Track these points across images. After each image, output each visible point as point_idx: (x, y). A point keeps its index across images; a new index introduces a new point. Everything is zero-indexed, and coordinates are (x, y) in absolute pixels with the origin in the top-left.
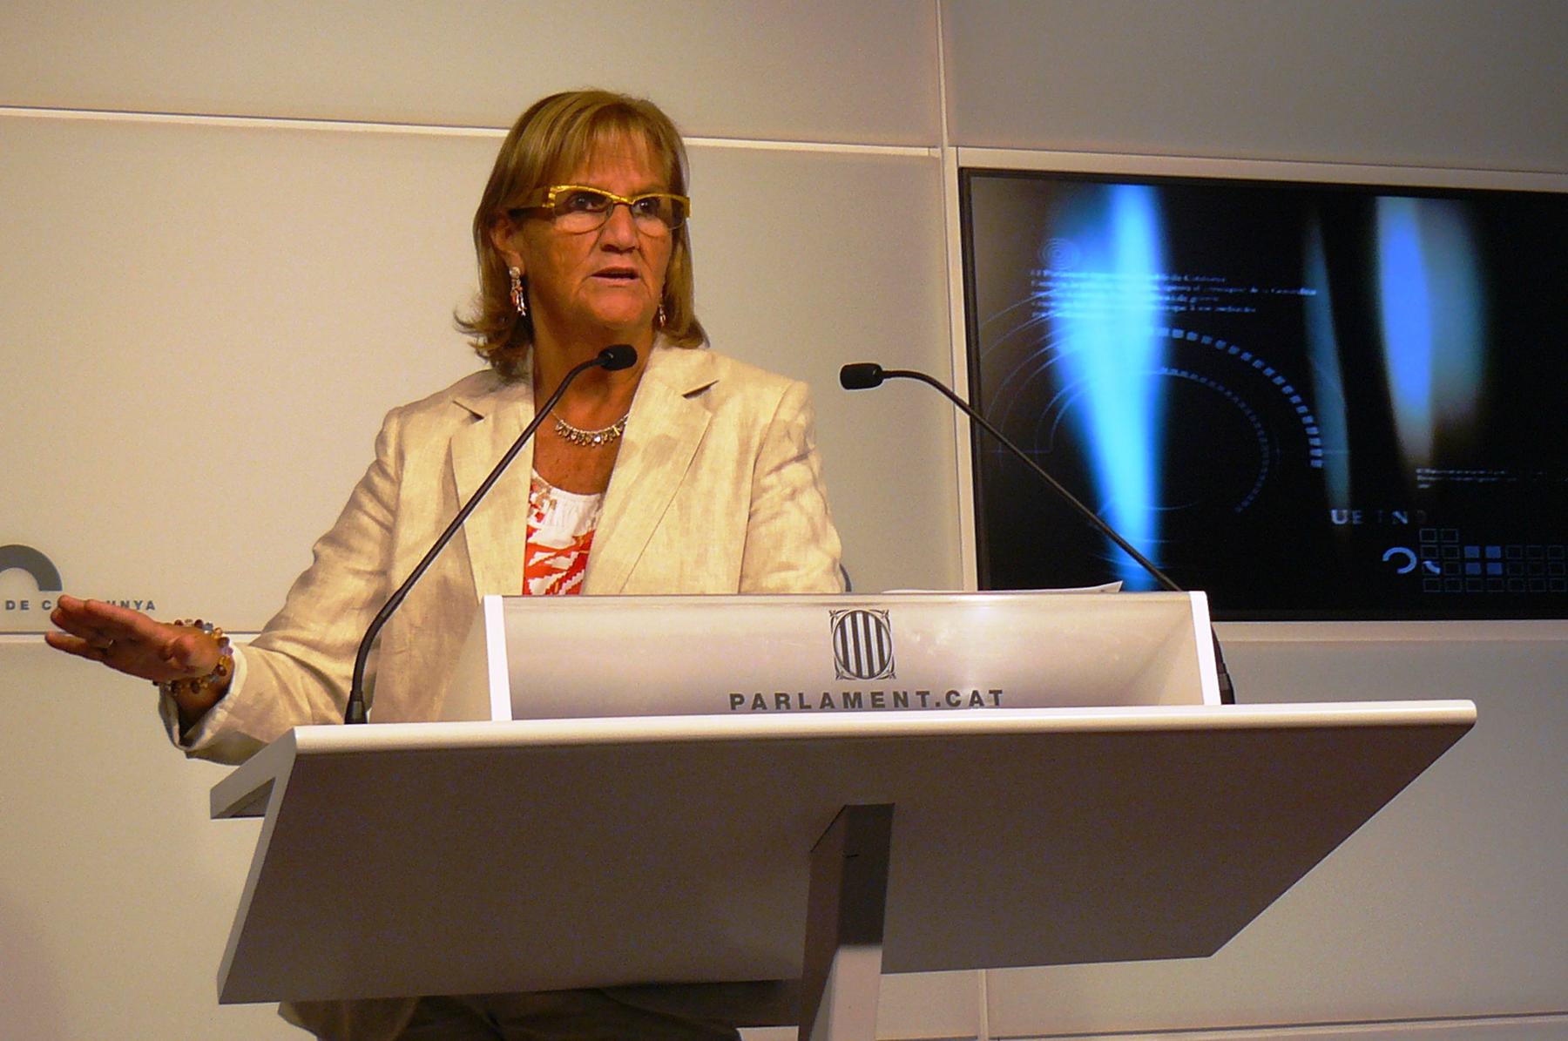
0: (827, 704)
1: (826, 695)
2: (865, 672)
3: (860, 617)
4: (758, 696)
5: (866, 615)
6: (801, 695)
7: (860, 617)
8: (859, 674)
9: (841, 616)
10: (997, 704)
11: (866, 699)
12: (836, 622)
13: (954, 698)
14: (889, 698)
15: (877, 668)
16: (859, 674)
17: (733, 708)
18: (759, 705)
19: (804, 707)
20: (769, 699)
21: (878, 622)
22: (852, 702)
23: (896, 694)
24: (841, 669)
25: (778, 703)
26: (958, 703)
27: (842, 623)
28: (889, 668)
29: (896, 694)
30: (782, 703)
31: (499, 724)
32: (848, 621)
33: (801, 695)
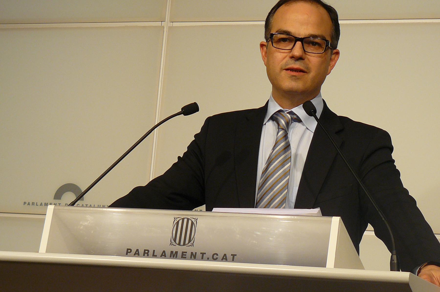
0: (163, 255)
1: (164, 252)
2: (182, 243)
3: (185, 220)
4: (137, 250)
5: (188, 220)
6: (154, 251)
7: (185, 220)
8: (179, 244)
10: (233, 260)
11: (180, 254)
13: (215, 257)
14: (188, 255)
15: (187, 242)
16: (179, 244)
17: (127, 254)
18: (137, 254)
19: (154, 256)
20: (141, 252)
21: (192, 223)
22: (174, 255)
23: (192, 253)
24: (173, 241)
25: (145, 253)
26: (217, 258)
27: (178, 223)
28: (192, 242)
29: (192, 253)
30: (146, 253)
31: (42, 254)
32: (180, 222)
33: (154, 251)
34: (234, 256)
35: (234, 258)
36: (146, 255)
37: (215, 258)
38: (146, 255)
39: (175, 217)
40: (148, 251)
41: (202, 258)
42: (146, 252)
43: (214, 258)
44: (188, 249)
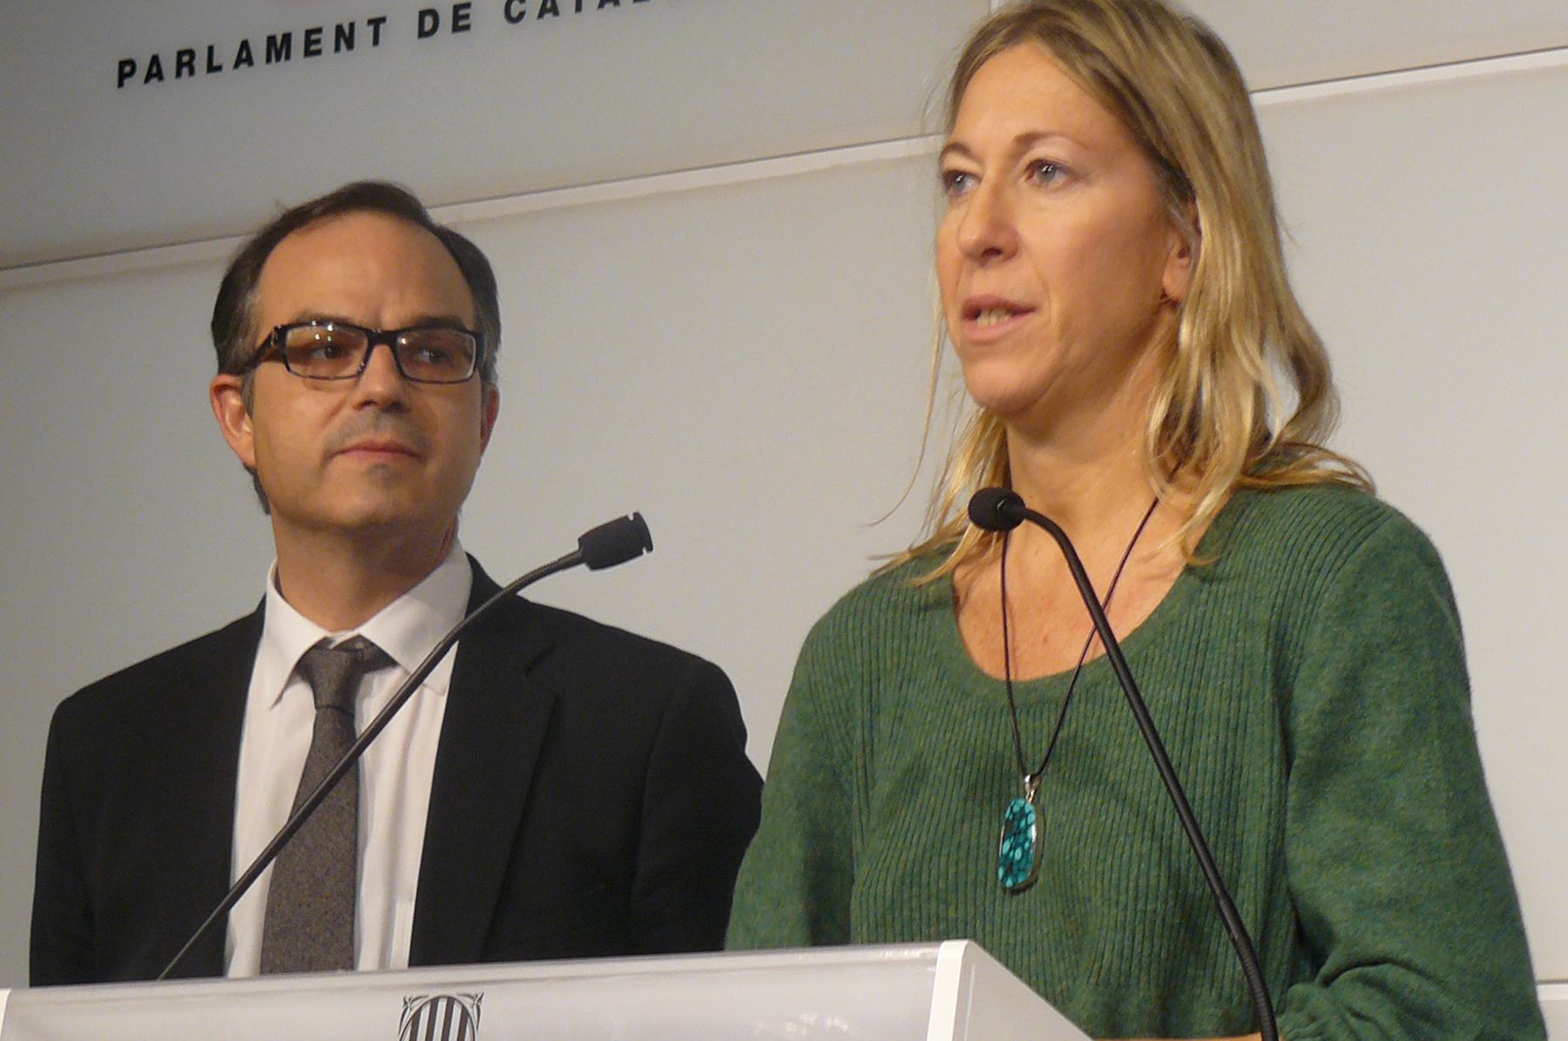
23: (339, 29)
42: (186, 59)
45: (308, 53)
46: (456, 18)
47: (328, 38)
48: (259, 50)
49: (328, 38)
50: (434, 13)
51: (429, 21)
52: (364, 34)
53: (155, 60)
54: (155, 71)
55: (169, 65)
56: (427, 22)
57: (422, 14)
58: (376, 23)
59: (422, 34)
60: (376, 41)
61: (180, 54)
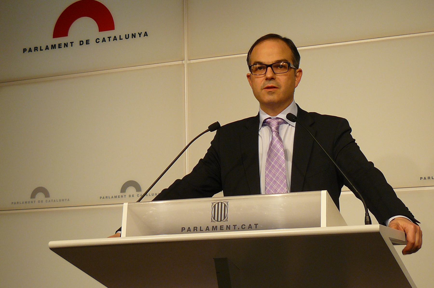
0: (207, 230)
1: (208, 227)
2: (219, 220)
3: (220, 204)
4: (189, 228)
5: (222, 203)
6: (201, 227)
7: (220, 204)
8: (218, 221)
9: (215, 204)
11: (219, 228)
12: (213, 205)
13: (243, 227)
14: (225, 227)
16: (218, 221)
18: (189, 231)
19: (201, 231)
20: (192, 229)
22: (215, 229)
23: (227, 226)
24: (213, 219)
25: (194, 229)
28: (226, 218)
29: (227, 226)
30: (195, 230)
33: (201, 227)
34: (256, 225)
35: (256, 227)
36: (195, 230)
37: (243, 227)
38: (195, 230)
39: (213, 202)
40: (197, 227)
41: (235, 229)
43: (243, 228)
44: (224, 224)
45: (59, 48)
46: (87, 42)
47: (63, 45)
48: (50, 47)
49: (63, 45)
50: (82, 41)
51: (82, 43)
52: (69, 45)
53: (30, 49)
54: (30, 50)
55: (33, 49)
56: (81, 43)
57: (80, 41)
58: (72, 43)
59: (80, 45)
60: (72, 46)
61: (35, 48)
